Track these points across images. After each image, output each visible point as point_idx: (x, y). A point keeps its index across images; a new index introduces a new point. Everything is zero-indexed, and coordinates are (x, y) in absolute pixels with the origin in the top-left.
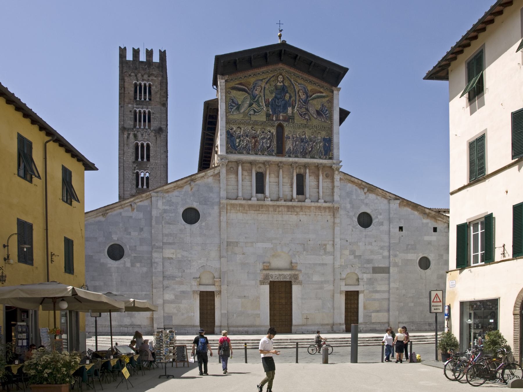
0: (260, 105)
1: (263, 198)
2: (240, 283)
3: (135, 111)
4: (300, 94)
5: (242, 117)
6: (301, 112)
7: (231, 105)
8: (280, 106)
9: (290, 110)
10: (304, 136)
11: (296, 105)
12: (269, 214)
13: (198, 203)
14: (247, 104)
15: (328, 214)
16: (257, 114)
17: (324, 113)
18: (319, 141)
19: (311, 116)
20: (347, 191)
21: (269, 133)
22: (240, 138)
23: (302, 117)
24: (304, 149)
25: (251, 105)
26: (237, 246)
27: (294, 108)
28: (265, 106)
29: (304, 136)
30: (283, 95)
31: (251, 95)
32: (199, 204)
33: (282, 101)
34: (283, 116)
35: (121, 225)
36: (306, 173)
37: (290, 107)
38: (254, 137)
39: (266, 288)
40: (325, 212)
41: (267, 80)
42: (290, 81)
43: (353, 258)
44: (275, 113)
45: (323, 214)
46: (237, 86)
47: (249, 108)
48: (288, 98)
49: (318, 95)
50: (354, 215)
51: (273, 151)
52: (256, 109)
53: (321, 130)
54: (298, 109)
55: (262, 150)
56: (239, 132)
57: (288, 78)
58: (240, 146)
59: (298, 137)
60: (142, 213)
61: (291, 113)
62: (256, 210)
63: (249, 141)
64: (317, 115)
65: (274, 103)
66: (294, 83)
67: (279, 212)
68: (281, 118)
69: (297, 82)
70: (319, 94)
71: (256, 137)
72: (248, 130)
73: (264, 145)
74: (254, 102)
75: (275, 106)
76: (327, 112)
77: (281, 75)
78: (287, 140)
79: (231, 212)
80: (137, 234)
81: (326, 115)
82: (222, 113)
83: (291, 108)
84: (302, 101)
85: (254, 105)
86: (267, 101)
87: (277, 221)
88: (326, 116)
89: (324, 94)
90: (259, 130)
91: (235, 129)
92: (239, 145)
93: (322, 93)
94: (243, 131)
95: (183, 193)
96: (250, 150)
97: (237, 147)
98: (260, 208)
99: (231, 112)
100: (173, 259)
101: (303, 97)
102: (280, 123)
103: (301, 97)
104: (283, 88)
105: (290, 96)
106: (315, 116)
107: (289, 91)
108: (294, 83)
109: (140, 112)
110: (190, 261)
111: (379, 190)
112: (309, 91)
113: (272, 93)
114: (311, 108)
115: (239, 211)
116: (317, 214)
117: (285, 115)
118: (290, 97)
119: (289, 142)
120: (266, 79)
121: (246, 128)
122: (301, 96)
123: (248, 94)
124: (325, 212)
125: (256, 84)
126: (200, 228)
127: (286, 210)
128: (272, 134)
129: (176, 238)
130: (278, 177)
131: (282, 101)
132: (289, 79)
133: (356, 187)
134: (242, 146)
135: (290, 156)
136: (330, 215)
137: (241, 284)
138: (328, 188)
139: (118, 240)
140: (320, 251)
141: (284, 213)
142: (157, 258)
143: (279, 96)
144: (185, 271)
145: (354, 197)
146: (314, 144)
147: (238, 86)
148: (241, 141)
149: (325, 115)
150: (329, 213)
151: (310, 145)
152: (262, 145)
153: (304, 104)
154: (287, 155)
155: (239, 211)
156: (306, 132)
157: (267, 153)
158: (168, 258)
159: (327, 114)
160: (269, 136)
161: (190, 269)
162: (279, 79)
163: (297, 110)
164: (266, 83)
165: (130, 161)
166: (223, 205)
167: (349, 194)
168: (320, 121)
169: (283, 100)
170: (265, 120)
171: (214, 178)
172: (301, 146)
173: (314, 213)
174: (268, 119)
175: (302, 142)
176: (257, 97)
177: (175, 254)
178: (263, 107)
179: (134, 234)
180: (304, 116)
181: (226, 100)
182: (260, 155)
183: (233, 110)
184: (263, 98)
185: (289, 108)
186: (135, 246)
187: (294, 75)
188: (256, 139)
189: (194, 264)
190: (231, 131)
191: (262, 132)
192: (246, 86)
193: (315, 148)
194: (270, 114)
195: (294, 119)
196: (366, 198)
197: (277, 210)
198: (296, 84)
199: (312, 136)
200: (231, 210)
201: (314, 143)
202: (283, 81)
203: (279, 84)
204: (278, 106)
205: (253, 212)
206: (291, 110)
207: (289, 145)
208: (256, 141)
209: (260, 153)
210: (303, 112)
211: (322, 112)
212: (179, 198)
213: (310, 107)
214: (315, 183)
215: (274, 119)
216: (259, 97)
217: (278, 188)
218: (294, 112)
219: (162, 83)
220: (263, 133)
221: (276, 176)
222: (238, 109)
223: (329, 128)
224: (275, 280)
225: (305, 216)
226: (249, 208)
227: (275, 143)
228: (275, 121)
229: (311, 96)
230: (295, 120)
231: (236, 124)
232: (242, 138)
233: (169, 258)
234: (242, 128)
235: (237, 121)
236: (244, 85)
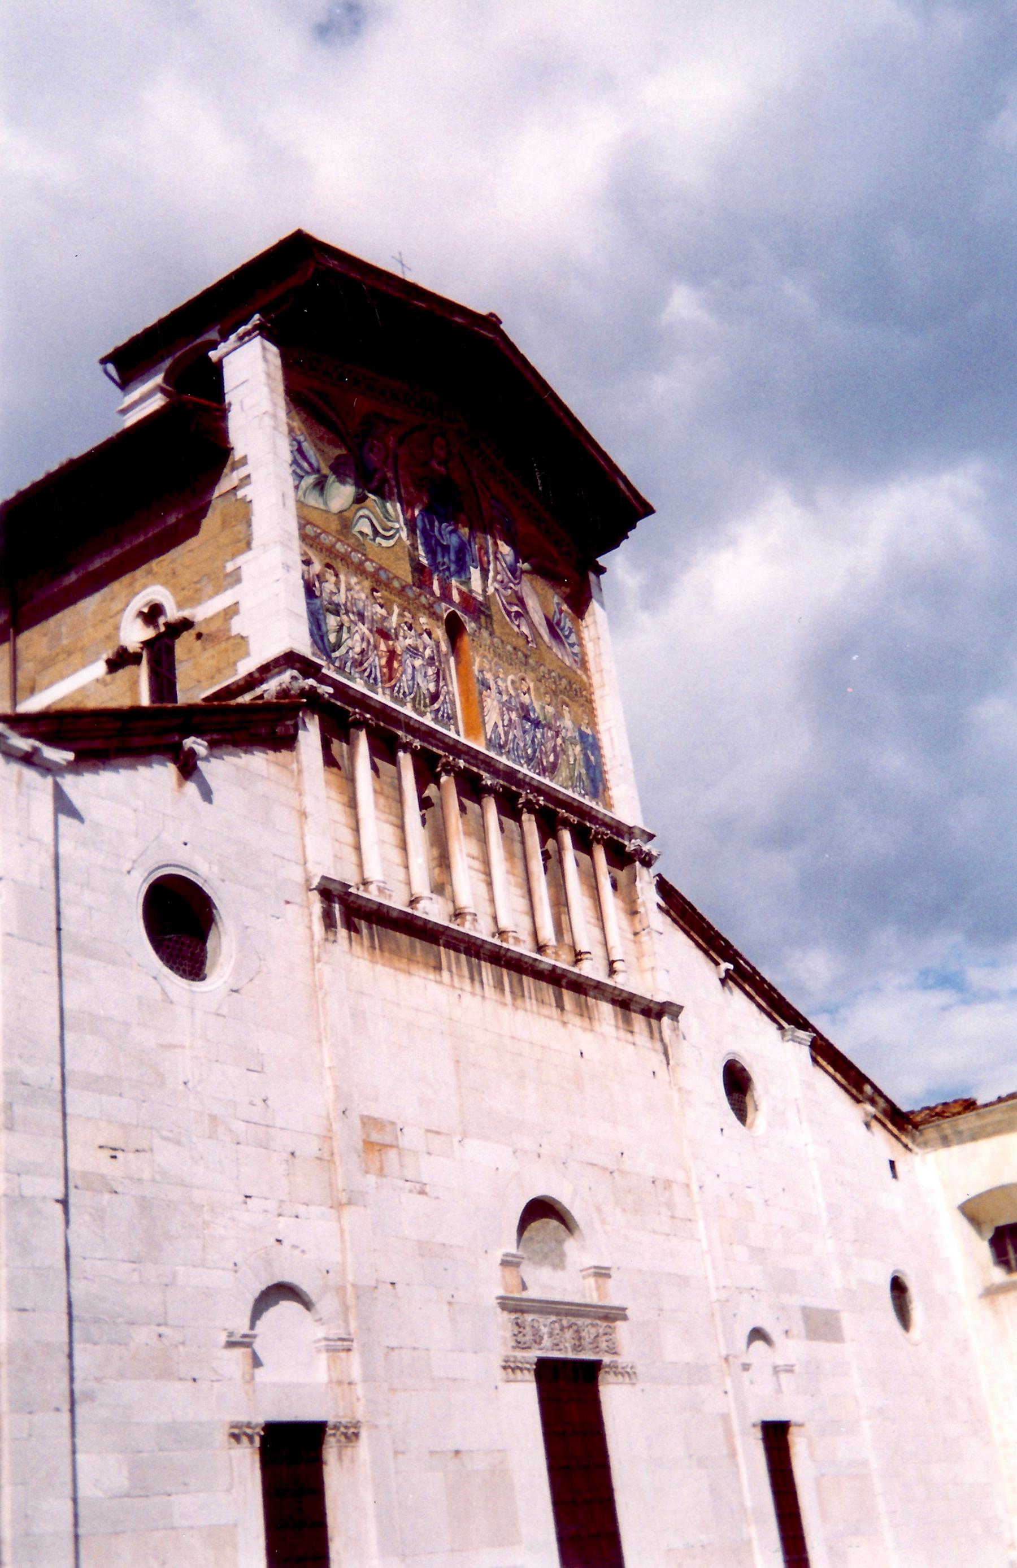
134: (347, 652)
152: (413, 678)
188: (391, 643)
194: (423, 566)
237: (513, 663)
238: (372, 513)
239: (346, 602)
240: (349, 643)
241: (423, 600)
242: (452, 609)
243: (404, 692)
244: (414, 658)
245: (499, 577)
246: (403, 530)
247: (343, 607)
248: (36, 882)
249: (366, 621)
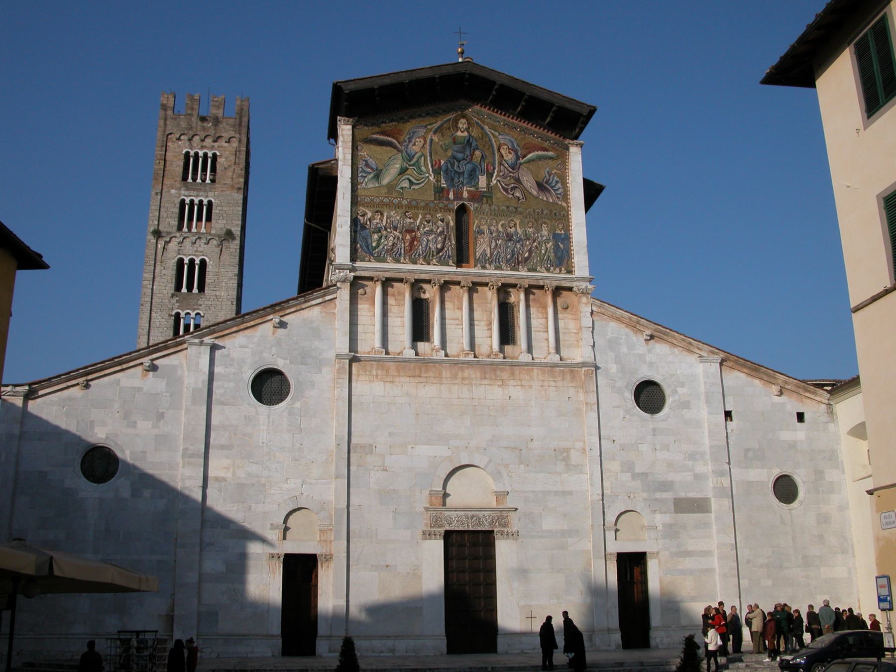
0: (422, 172)
1: (430, 352)
2: (377, 535)
3: (183, 201)
4: (503, 152)
5: (385, 193)
6: (506, 185)
7: (363, 171)
8: (463, 173)
9: (482, 181)
10: (513, 230)
11: (496, 171)
12: (441, 384)
13: (288, 361)
14: (396, 170)
15: (570, 385)
16: (416, 187)
17: (552, 187)
18: (544, 238)
19: (526, 191)
20: (608, 337)
21: (440, 222)
22: (380, 231)
23: (507, 192)
24: (513, 256)
25: (403, 171)
26: (371, 453)
27: (492, 176)
28: (432, 172)
29: (513, 230)
30: (468, 153)
31: (404, 153)
32: (290, 362)
33: (466, 164)
34: (469, 192)
35: (117, 406)
36: (519, 303)
37: (484, 175)
38: (410, 231)
39: (438, 546)
40: (563, 380)
41: (436, 126)
42: (482, 128)
43: (630, 479)
44: (454, 186)
45: (560, 384)
46: (375, 136)
47: (400, 176)
48: (479, 159)
49: (539, 155)
50: (626, 387)
51: (449, 257)
52: (413, 177)
53: (548, 219)
54: (498, 179)
55: (426, 254)
56: (378, 221)
57: (477, 123)
58: (381, 247)
59: (500, 232)
60: (165, 382)
61: (485, 186)
62: (414, 377)
63: (399, 238)
64: (539, 190)
65: (450, 167)
66: (491, 133)
67: (463, 379)
68: (465, 195)
69: (495, 130)
70: (540, 153)
71: (414, 231)
72: (398, 218)
73: (431, 246)
74: (409, 165)
75: (453, 174)
76: (559, 185)
77: (464, 117)
78: (479, 237)
79: (360, 379)
80: (150, 426)
81: (557, 190)
82: (345, 185)
83: (485, 177)
84: (506, 165)
85: (408, 172)
86: (436, 164)
87: (459, 398)
88: (557, 192)
89: (550, 153)
90: (420, 216)
91: (369, 215)
92: (378, 246)
93: (547, 150)
94: (387, 218)
95: (256, 340)
96: (400, 255)
97: (375, 249)
98: (423, 371)
99: (362, 183)
100: (226, 481)
101: (509, 157)
102: (463, 204)
103: (505, 158)
104: (469, 139)
105: (482, 156)
106: (535, 193)
107: (480, 147)
108: (491, 133)
109: (192, 201)
110: (264, 485)
111: (676, 334)
112: (521, 147)
113: (446, 150)
114: (525, 178)
115: (377, 378)
116: (546, 384)
117: (472, 189)
118: (483, 157)
119: (482, 240)
120: (434, 125)
121: (392, 213)
122: (504, 155)
123: (399, 151)
124: (563, 380)
125: (414, 132)
126: (290, 413)
127: (478, 375)
128: (448, 224)
129: (235, 434)
130: (460, 308)
131: (466, 164)
132: (480, 126)
133: (628, 330)
134: (384, 247)
135: (484, 267)
136: (575, 387)
137: (378, 538)
138: (567, 331)
139: (107, 437)
140: (556, 464)
141: (474, 382)
142: (190, 478)
143: (460, 156)
144: (252, 508)
145: (624, 350)
146: (535, 244)
147: (378, 136)
148: (383, 237)
149: (554, 190)
150: (572, 382)
151: (526, 245)
152: (427, 245)
153: (510, 170)
154: (479, 265)
155: (377, 378)
156: (518, 223)
157: (437, 261)
158: (216, 477)
159: (560, 188)
160: (440, 229)
161: (264, 503)
162: (460, 126)
163: (498, 181)
164: (435, 133)
165: (165, 292)
166: (341, 365)
167: (613, 344)
168: (545, 203)
169: (468, 163)
170: (433, 199)
171: (325, 309)
172: (507, 248)
173: (541, 383)
174: (439, 196)
175: (510, 240)
176: (417, 156)
177: (231, 470)
178: (427, 175)
179: (144, 426)
180: (511, 191)
181: (352, 162)
182: (422, 264)
183: (366, 180)
184: (429, 158)
185: (480, 177)
186: (145, 452)
187: (490, 118)
188: (414, 234)
189: (273, 491)
190: (361, 218)
191: (426, 221)
192: (394, 138)
193: (536, 253)
194: (443, 189)
195: (491, 197)
196: (649, 351)
197: (460, 375)
198: (493, 135)
199: (531, 230)
200: (358, 375)
201: (534, 241)
202: (469, 128)
203: (459, 134)
204: (459, 173)
205: (407, 379)
206: (485, 182)
207: (481, 246)
208: (414, 239)
209: (421, 260)
210: (509, 185)
211: (548, 185)
212: (247, 350)
213: (523, 175)
214: (539, 320)
215: (451, 196)
216: (421, 157)
217: (460, 330)
218: (492, 184)
219: (237, 153)
220: (428, 222)
221: (456, 307)
222: (378, 178)
223: (564, 215)
224: (456, 529)
225: (519, 387)
226: (398, 371)
227: (454, 242)
228: (454, 200)
229: (525, 156)
230: (494, 200)
231: (374, 206)
232: (385, 232)
233: (217, 479)
234: (385, 214)
235: (375, 200)
236: (389, 136)
237: (505, 215)
238: (411, 176)
239: (386, 225)
240: (386, 242)
241: (441, 205)
242: (462, 202)
243: (419, 254)
244: (429, 236)
245: (501, 174)
246: (431, 176)
247: (383, 228)
248: (200, 386)
249: (398, 229)
